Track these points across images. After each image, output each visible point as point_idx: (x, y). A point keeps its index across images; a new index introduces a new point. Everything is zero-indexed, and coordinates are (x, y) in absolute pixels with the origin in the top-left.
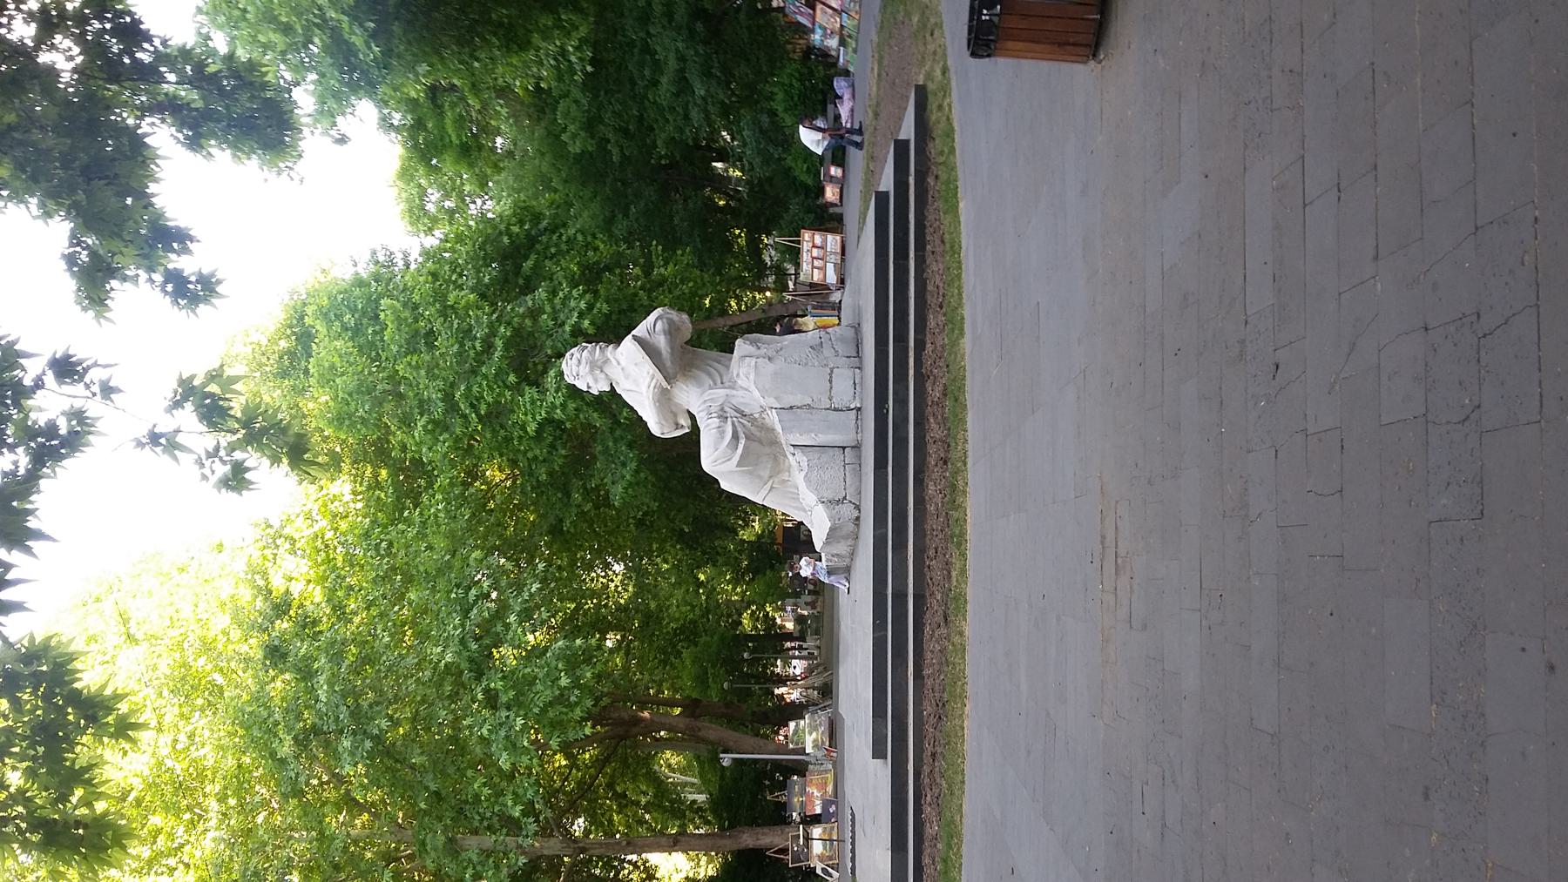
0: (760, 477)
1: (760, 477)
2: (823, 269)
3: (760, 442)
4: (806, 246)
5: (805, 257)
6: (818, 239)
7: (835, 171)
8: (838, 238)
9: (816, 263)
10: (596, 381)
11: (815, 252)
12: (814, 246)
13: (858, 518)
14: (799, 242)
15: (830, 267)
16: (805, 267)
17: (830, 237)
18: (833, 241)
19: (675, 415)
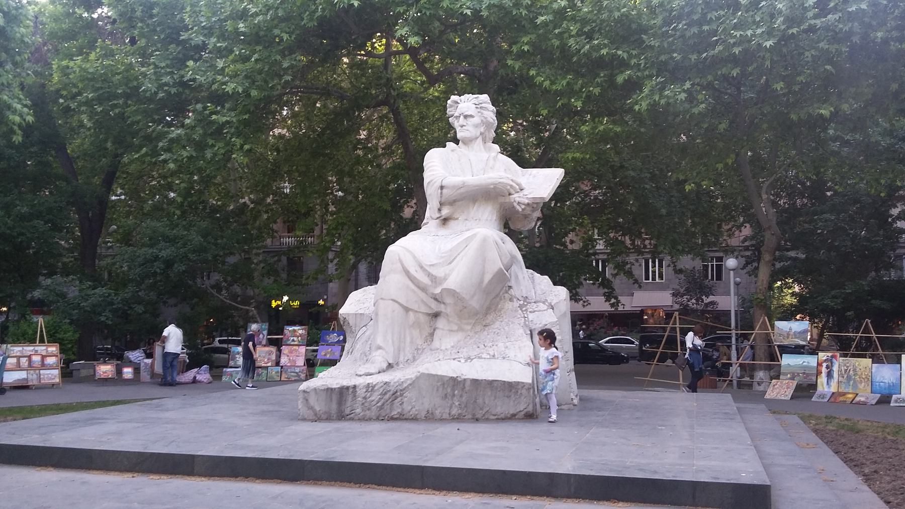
0: (473, 296)
1: (473, 296)
2: (18, 367)
3: (497, 296)
4: (41, 349)
5: (29, 349)
6: (51, 360)
7: (128, 372)
8: (57, 380)
9: (24, 361)
10: (476, 126)
11: (36, 359)
12: (43, 357)
13: (530, 417)
14: (42, 341)
15: (22, 375)
16: (17, 350)
17: (56, 372)
18: (53, 375)
19: (452, 203)
